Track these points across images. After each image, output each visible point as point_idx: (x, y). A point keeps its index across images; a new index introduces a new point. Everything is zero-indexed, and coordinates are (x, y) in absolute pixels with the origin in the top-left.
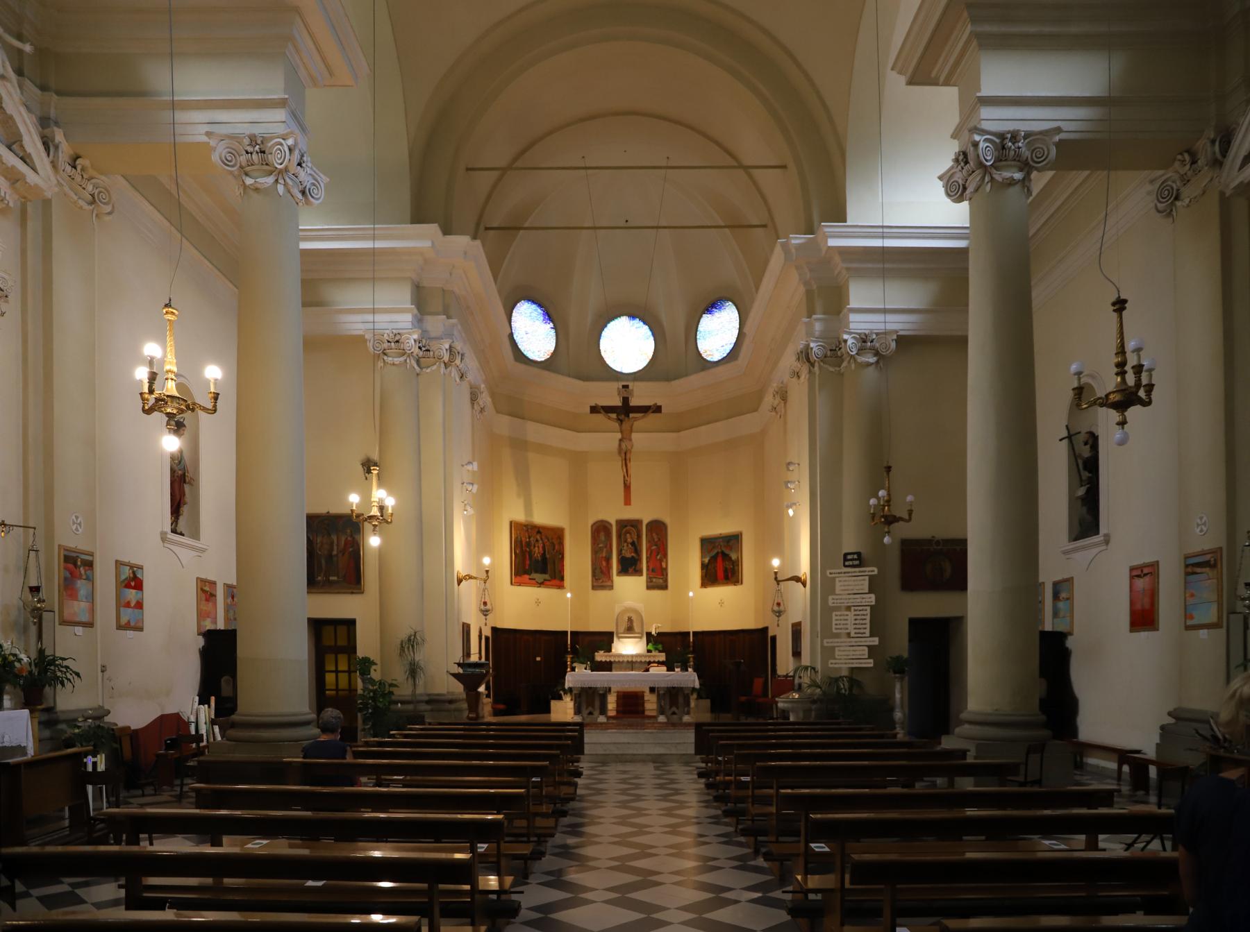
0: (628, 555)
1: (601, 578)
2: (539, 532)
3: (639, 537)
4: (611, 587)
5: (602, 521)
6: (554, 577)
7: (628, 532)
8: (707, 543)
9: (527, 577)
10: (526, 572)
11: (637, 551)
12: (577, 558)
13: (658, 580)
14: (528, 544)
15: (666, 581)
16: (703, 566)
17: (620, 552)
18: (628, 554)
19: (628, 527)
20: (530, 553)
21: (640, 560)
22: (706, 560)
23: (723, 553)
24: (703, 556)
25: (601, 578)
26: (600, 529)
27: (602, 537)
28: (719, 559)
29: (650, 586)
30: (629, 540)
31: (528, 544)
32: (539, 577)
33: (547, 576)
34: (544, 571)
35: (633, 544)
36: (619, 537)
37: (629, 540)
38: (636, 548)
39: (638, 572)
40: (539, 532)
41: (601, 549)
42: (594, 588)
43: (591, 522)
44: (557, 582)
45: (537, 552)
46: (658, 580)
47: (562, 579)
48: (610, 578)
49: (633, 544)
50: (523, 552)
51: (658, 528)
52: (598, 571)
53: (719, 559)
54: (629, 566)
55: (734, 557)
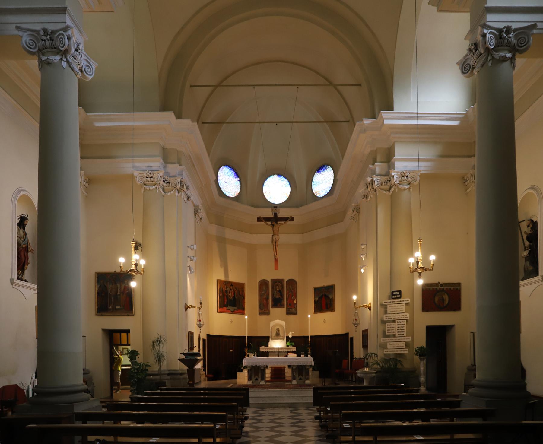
1: (264, 310)
2: (232, 285)
3: (283, 288)
5: (264, 280)
6: (239, 309)
8: (317, 291)
9: (225, 308)
10: (225, 306)
12: (251, 299)
13: (292, 310)
14: (226, 291)
16: (316, 302)
17: (273, 295)
18: (278, 296)
19: (277, 283)
20: (227, 296)
21: (283, 299)
22: (317, 299)
25: (264, 310)
26: (263, 284)
30: (278, 289)
33: (236, 308)
34: (234, 305)
35: (280, 291)
36: (273, 287)
37: (278, 289)
39: (282, 306)
42: (260, 314)
44: (241, 311)
45: (231, 295)
46: (292, 310)
47: (244, 309)
49: (280, 291)
51: (292, 283)
54: (277, 303)
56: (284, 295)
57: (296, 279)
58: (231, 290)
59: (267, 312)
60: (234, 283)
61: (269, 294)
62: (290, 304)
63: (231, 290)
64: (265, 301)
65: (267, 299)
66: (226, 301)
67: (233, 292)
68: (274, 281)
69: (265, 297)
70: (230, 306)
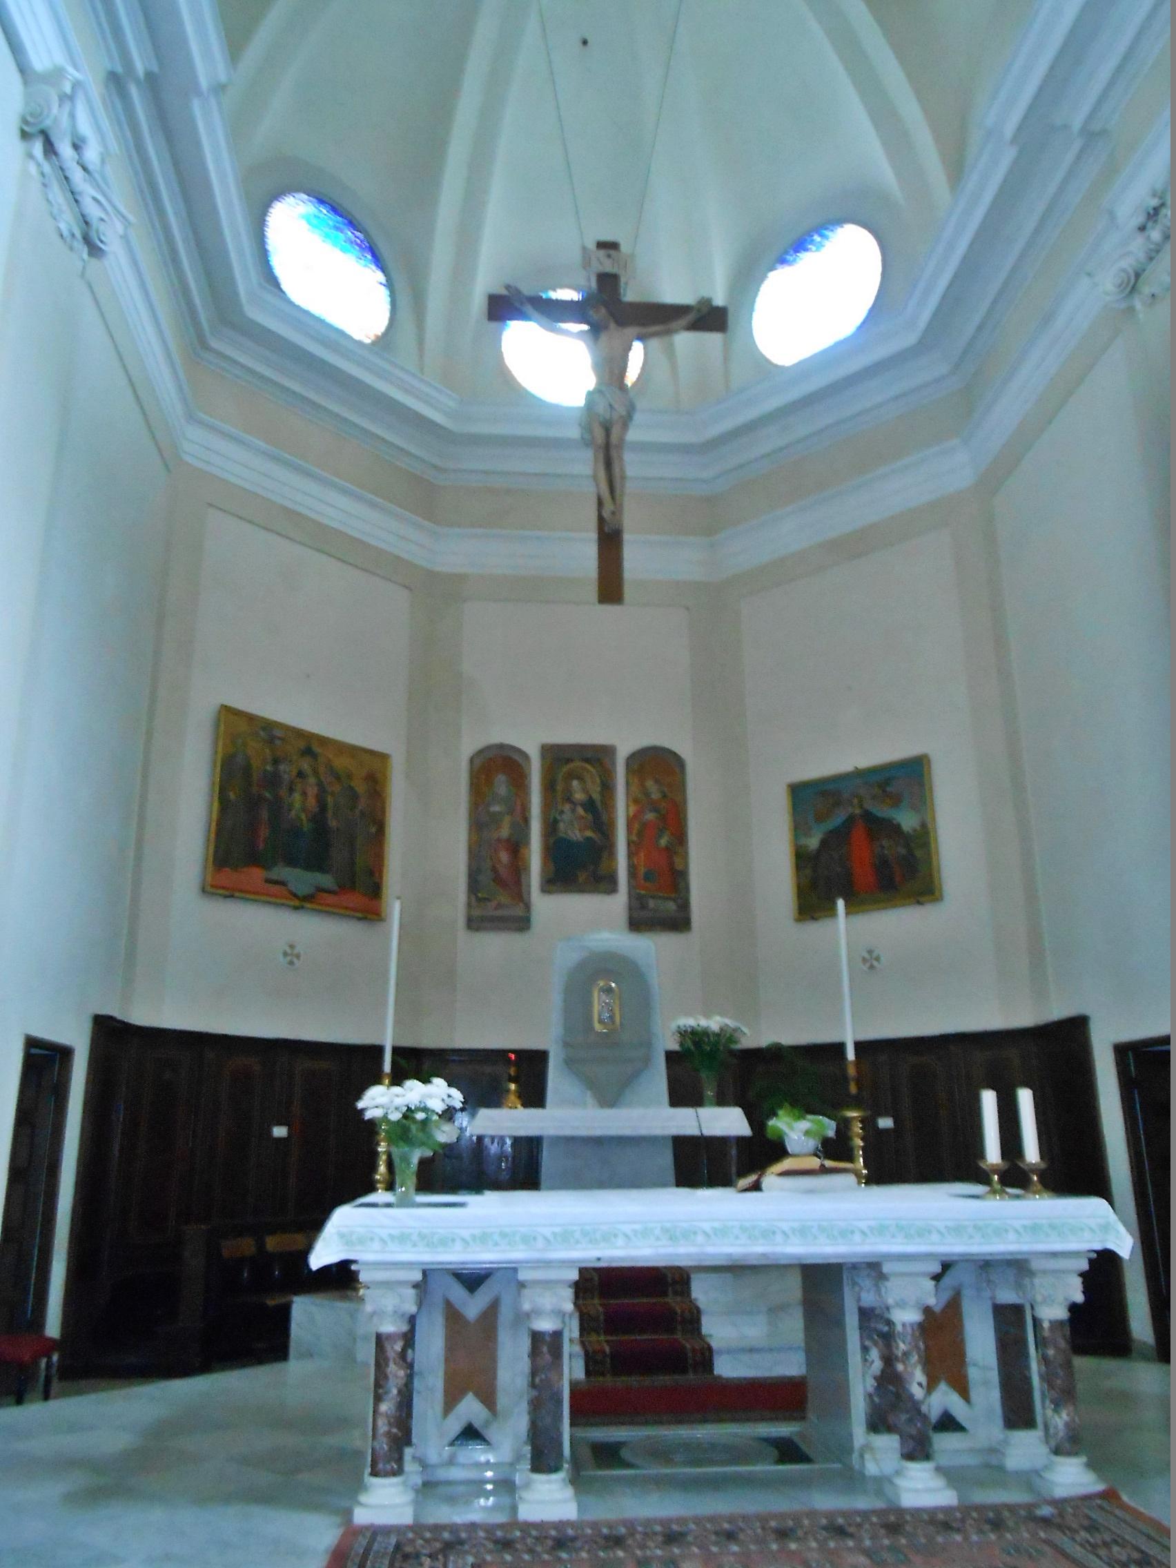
1: (496, 896)
2: (308, 752)
3: (607, 788)
4: (522, 923)
5: (501, 746)
6: (348, 883)
7: (571, 776)
8: (809, 798)
9: (256, 875)
10: (254, 858)
11: (604, 828)
12: (425, 842)
13: (662, 903)
14: (273, 780)
15: (685, 906)
16: (802, 858)
17: (550, 827)
18: (575, 831)
19: (574, 763)
20: (277, 808)
22: (813, 842)
23: (868, 816)
24: (799, 828)
25: (496, 896)
26: (496, 767)
27: (501, 785)
28: (859, 833)
29: (638, 922)
30: (579, 796)
31: (273, 780)
32: (300, 879)
33: (326, 880)
34: (317, 862)
35: (590, 805)
36: (549, 787)
37: (579, 796)
38: (598, 814)
39: (604, 883)
40: (308, 752)
41: (495, 819)
42: (474, 924)
43: (469, 745)
45: (300, 805)
46: (662, 903)
47: (375, 891)
48: (519, 894)
49: (590, 805)
50: (252, 803)
51: (658, 766)
52: (485, 878)
53: (859, 833)
54: (577, 867)
55: (907, 821)
56: (612, 824)
57: (682, 745)
58: (301, 774)
59: (519, 911)
60: (324, 741)
61: (526, 820)
63: (301, 774)
64: (504, 857)
65: (516, 846)
67: (312, 791)
68: (560, 758)
69: (505, 832)
70: (292, 862)
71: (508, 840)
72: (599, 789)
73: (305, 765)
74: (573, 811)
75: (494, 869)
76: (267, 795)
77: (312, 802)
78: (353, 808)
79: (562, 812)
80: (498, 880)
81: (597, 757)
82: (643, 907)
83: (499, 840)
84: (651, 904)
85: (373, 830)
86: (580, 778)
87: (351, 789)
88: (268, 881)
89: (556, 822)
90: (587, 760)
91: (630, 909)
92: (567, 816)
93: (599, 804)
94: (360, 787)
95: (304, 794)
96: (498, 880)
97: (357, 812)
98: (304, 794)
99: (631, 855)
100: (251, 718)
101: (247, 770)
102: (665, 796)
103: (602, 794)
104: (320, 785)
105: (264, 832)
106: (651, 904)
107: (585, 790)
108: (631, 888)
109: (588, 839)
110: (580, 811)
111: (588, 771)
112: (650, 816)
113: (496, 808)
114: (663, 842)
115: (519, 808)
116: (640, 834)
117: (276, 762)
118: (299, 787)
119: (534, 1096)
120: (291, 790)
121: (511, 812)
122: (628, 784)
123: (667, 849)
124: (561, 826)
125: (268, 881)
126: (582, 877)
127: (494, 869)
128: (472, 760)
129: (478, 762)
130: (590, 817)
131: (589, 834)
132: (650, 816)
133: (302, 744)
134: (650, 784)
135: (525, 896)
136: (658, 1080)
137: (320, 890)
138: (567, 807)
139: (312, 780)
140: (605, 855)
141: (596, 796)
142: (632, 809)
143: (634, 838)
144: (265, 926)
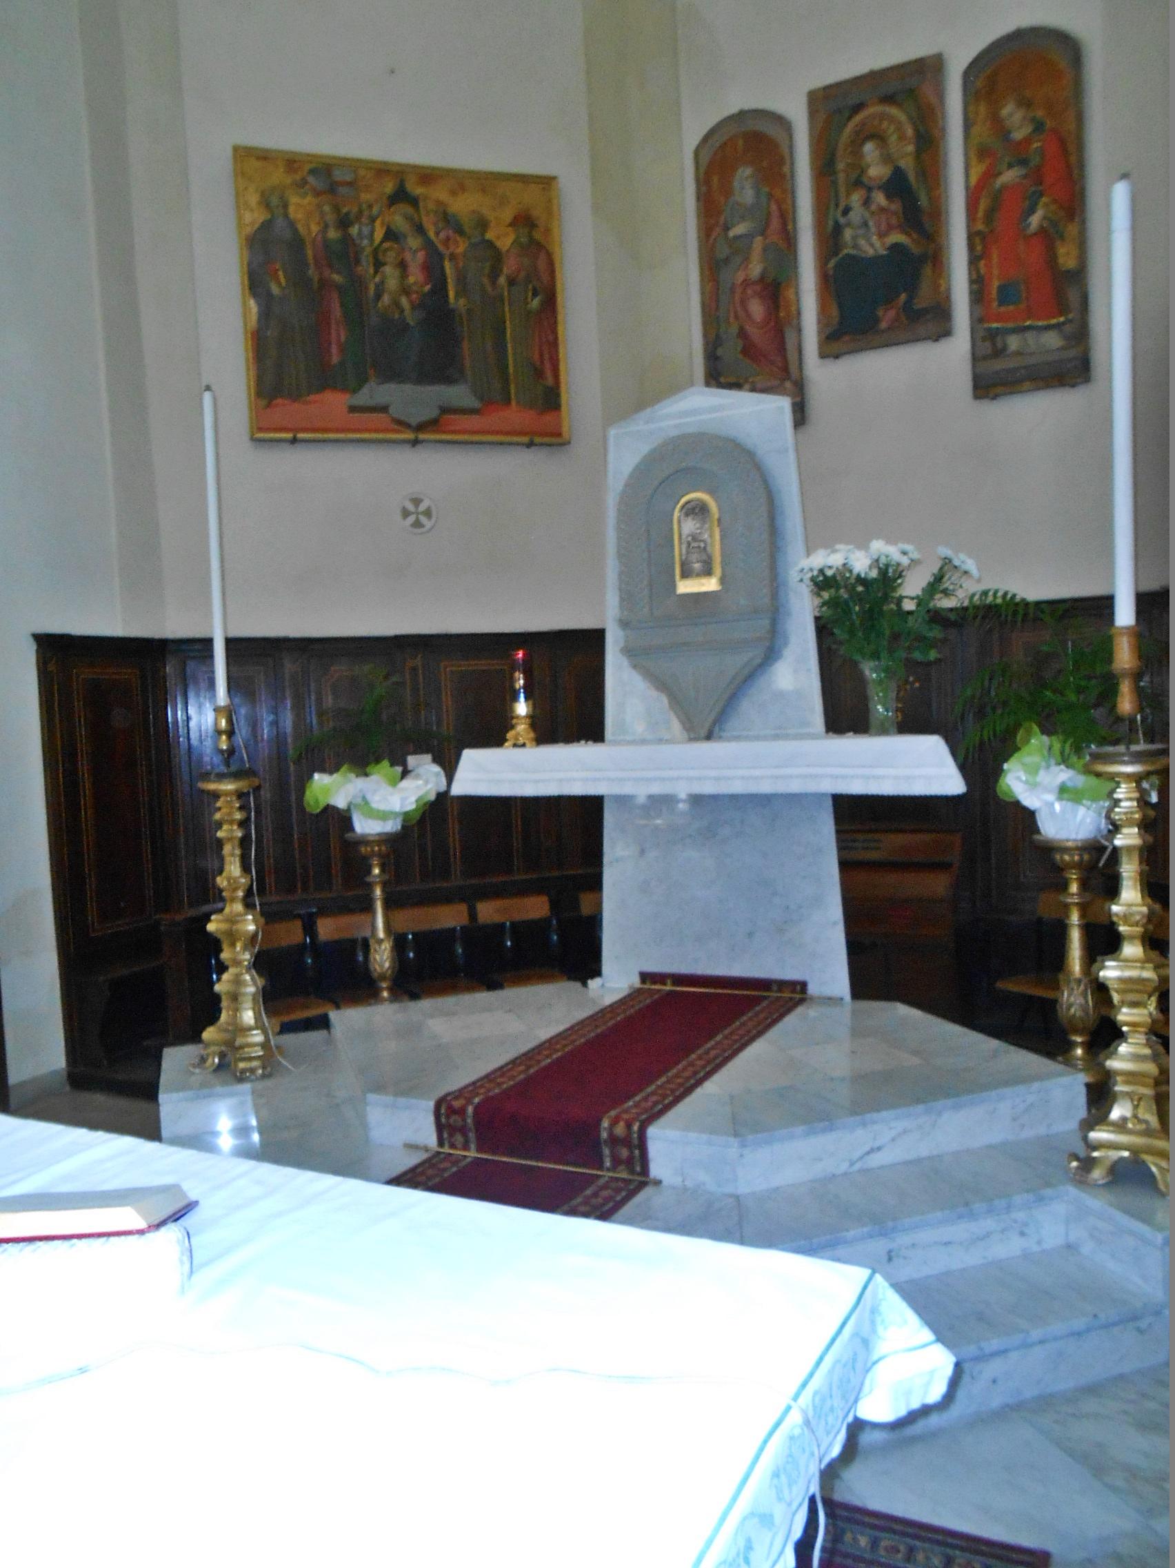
0: (872, 244)
3: (928, 142)
5: (741, 116)
6: (494, 397)
9: (335, 402)
14: (344, 253)
17: (830, 240)
21: (935, 257)
30: (877, 171)
31: (344, 253)
33: (459, 394)
35: (897, 186)
36: (824, 168)
38: (912, 199)
39: (931, 321)
40: (401, 196)
41: (741, 248)
44: (515, 415)
45: (396, 286)
47: (551, 400)
49: (897, 186)
54: (881, 300)
56: (938, 213)
58: (391, 235)
60: (428, 176)
62: (1005, 295)
64: (757, 309)
65: (775, 290)
66: (339, 334)
67: (415, 261)
68: (837, 106)
70: (391, 374)
71: (762, 278)
72: (910, 148)
73: (398, 218)
74: (867, 202)
75: (742, 334)
76: (337, 278)
77: (415, 276)
78: (494, 274)
79: (846, 211)
80: (749, 350)
81: (907, 87)
82: (998, 353)
83: (746, 283)
84: (1013, 342)
85: (535, 303)
86: (879, 138)
87: (490, 245)
88: (353, 409)
89: (838, 229)
90: (889, 99)
91: (975, 359)
92: (856, 215)
93: (912, 177)
94: (505, 240)
95: (402, 266)
96: (749, 350)
97: (502, 280)
98: (402, 266)
99: (973, 261)
100: (292, 162)
101: (297, 244)
102: (1039, 127)
103: (918, 153)
104: (429, 245)
105: (339, 334)
106: (1013, 342)
107: (887, 159)
108: (977, 321)
109: (895, 247)
110: (880, 199)
111: (892, 119)
112: (1009, 176)
113: (739, 229)
114: (1035, 220)
115: (775, 223)
116: (989, 217)
117: (344, 223)
118: (391, 257)
119: (575, 715)
120: (378, 265)
121: (763, 233)
122: (968, 125)
123: (1042, 231)
124: (848, 234)
125: (353, 409)
126: (887, 317)
127: (742, 334)
128: (697, 153)
129: (705, 159)
130: (896, 206)
131: (897, 237)
132: (1009, 176)
133: (389, 187)
134: (1011, 112)
135: (793, 368)
136: (797, 674)
137: (445, 410)
138: (856, 198)
139: (414, 242)
140: (927, 270)
141: (907, 164)
142: (977, 171)
143: (980, 226)
144: (363, 478)
